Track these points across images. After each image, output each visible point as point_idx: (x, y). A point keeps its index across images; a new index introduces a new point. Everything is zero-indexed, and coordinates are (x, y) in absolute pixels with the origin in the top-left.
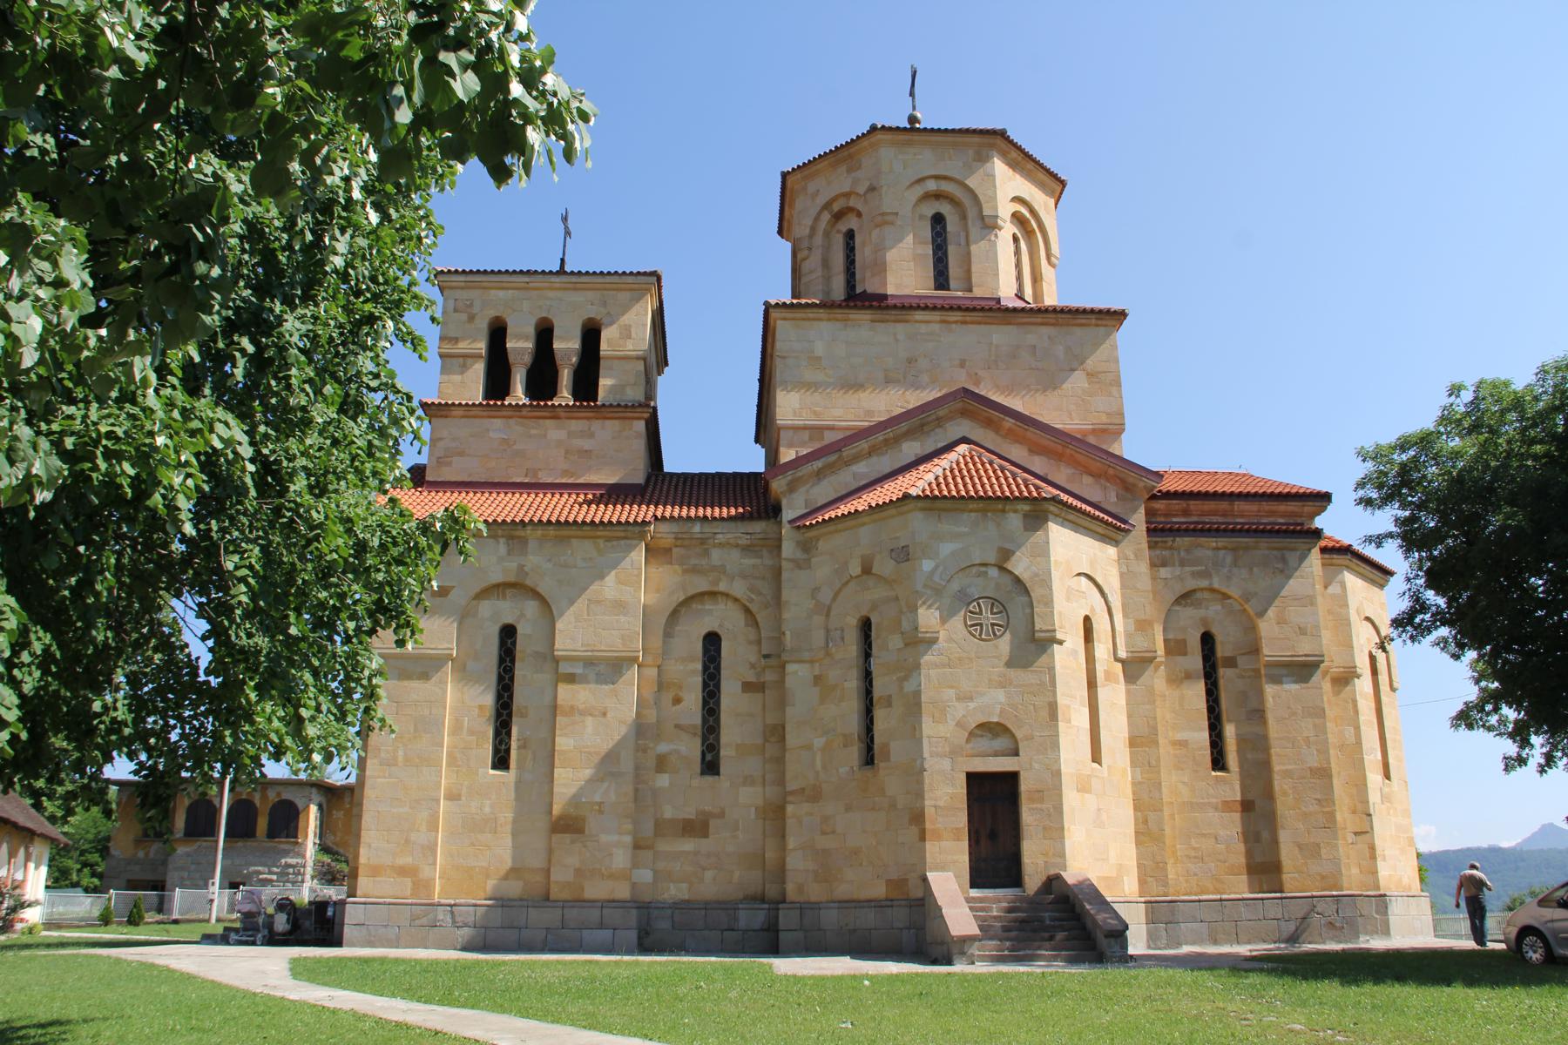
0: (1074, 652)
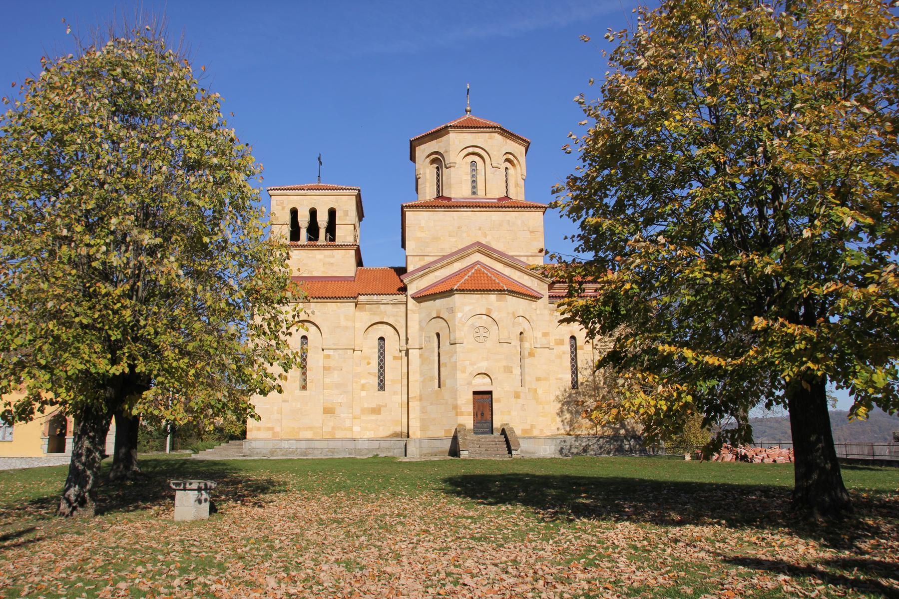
0: (515, 346)
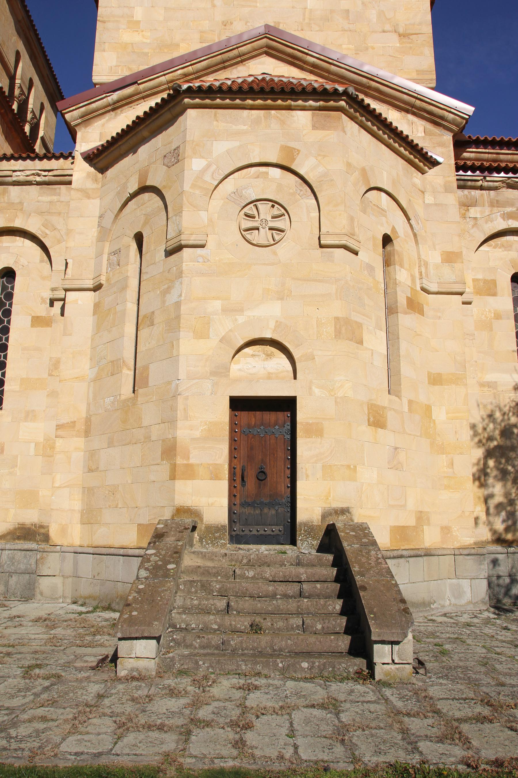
0: (371, 269)
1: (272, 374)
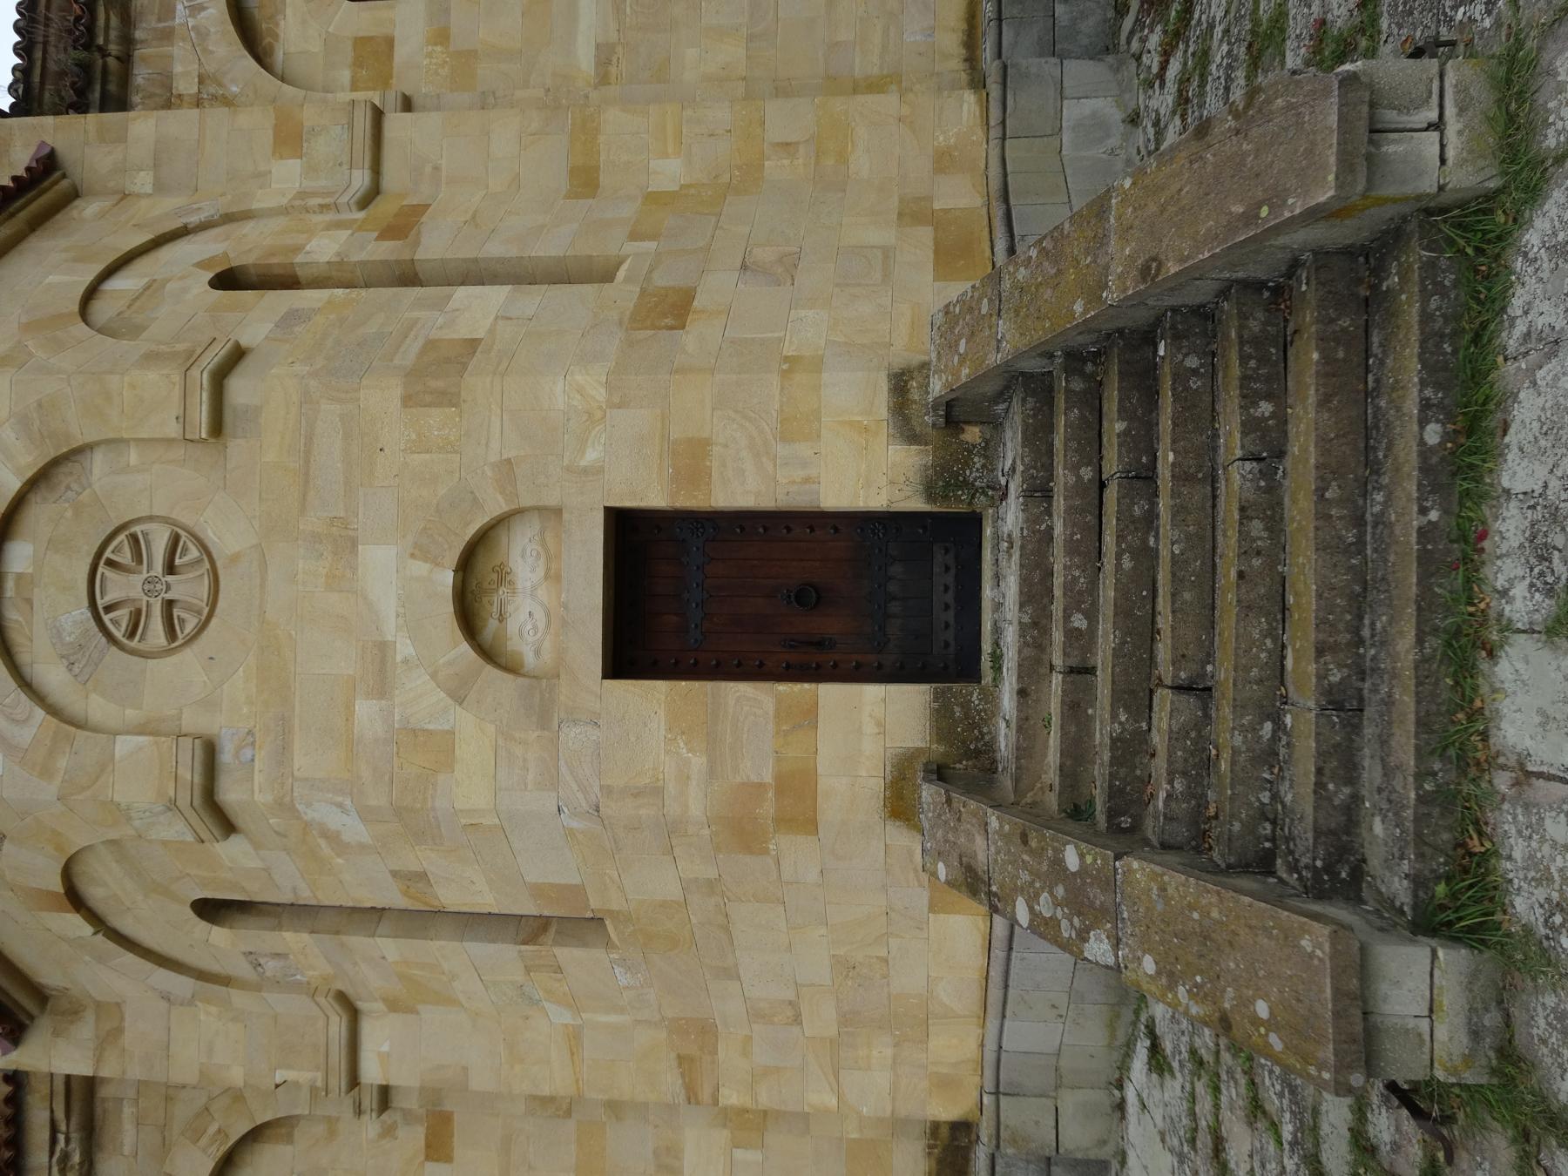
1: (548, 570)
